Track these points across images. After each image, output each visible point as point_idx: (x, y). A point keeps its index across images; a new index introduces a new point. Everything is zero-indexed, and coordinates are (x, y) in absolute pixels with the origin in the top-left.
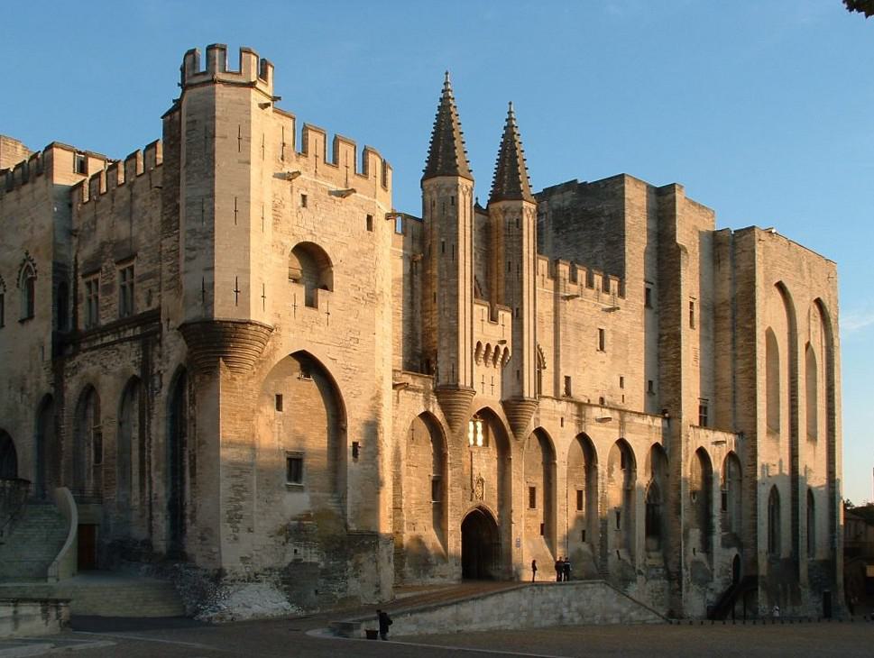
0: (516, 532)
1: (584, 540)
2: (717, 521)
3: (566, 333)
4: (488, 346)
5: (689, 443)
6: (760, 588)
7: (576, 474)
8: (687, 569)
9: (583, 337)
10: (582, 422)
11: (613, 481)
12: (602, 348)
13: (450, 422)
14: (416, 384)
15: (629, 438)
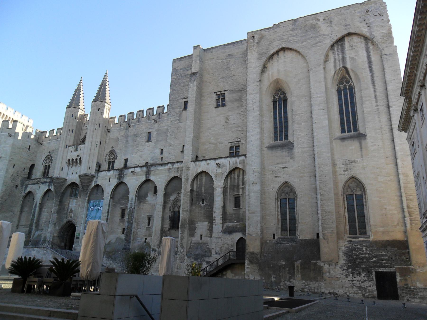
0: (78, 230)
1: (123, 233)
2: (218, 216)
3: (127, 141)
4: (73, 159)
5: (190, 172)
6: (247, 262)
7: (122, 202)
8: (182, 247)
9: (138, 139)
10: (121, 177)
11: (148, 201)
12: (149, 140)
13: (55, 190)
14: (47, 181)
15: (152, 178)
